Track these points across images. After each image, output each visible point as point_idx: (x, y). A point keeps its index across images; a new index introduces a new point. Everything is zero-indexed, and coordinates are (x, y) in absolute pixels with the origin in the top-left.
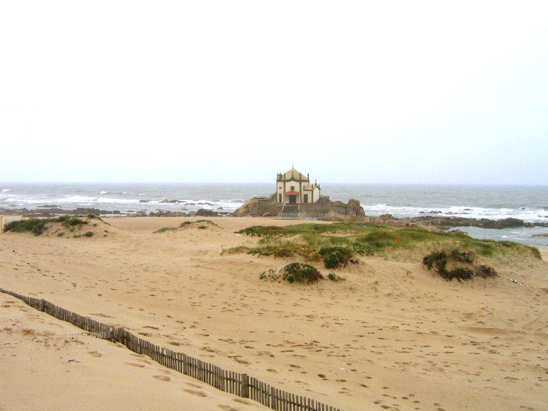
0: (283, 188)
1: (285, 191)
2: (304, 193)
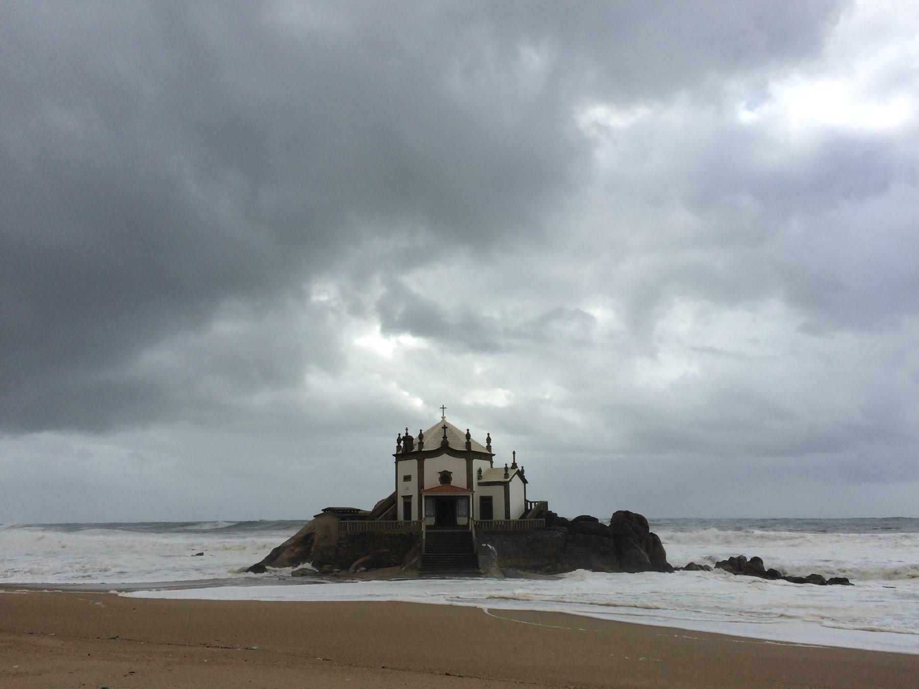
0: (415, 479)
1: (421, 485)
2: (478, 492)
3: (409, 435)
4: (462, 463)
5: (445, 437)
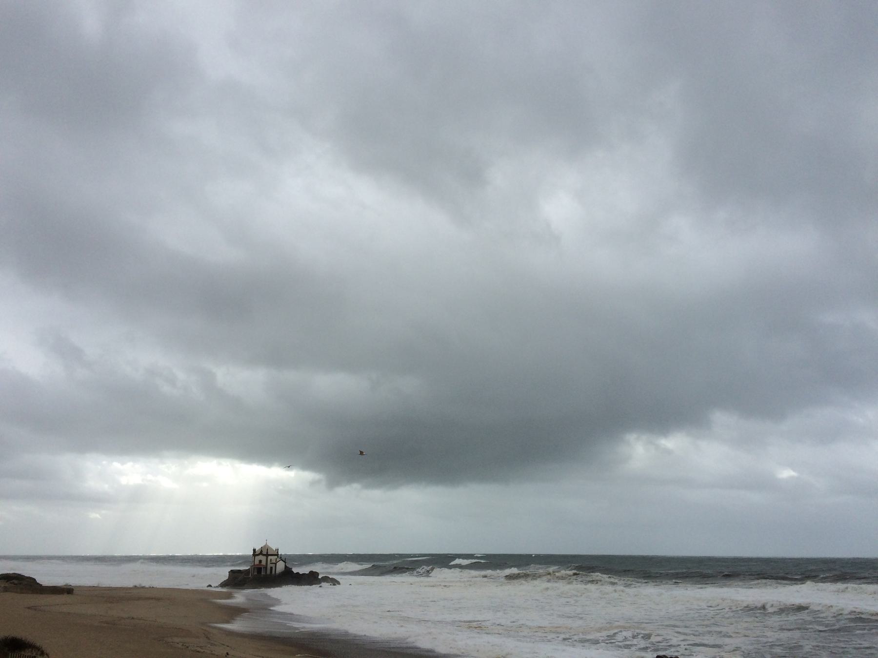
2: (269, 566)
4: (265, 557)
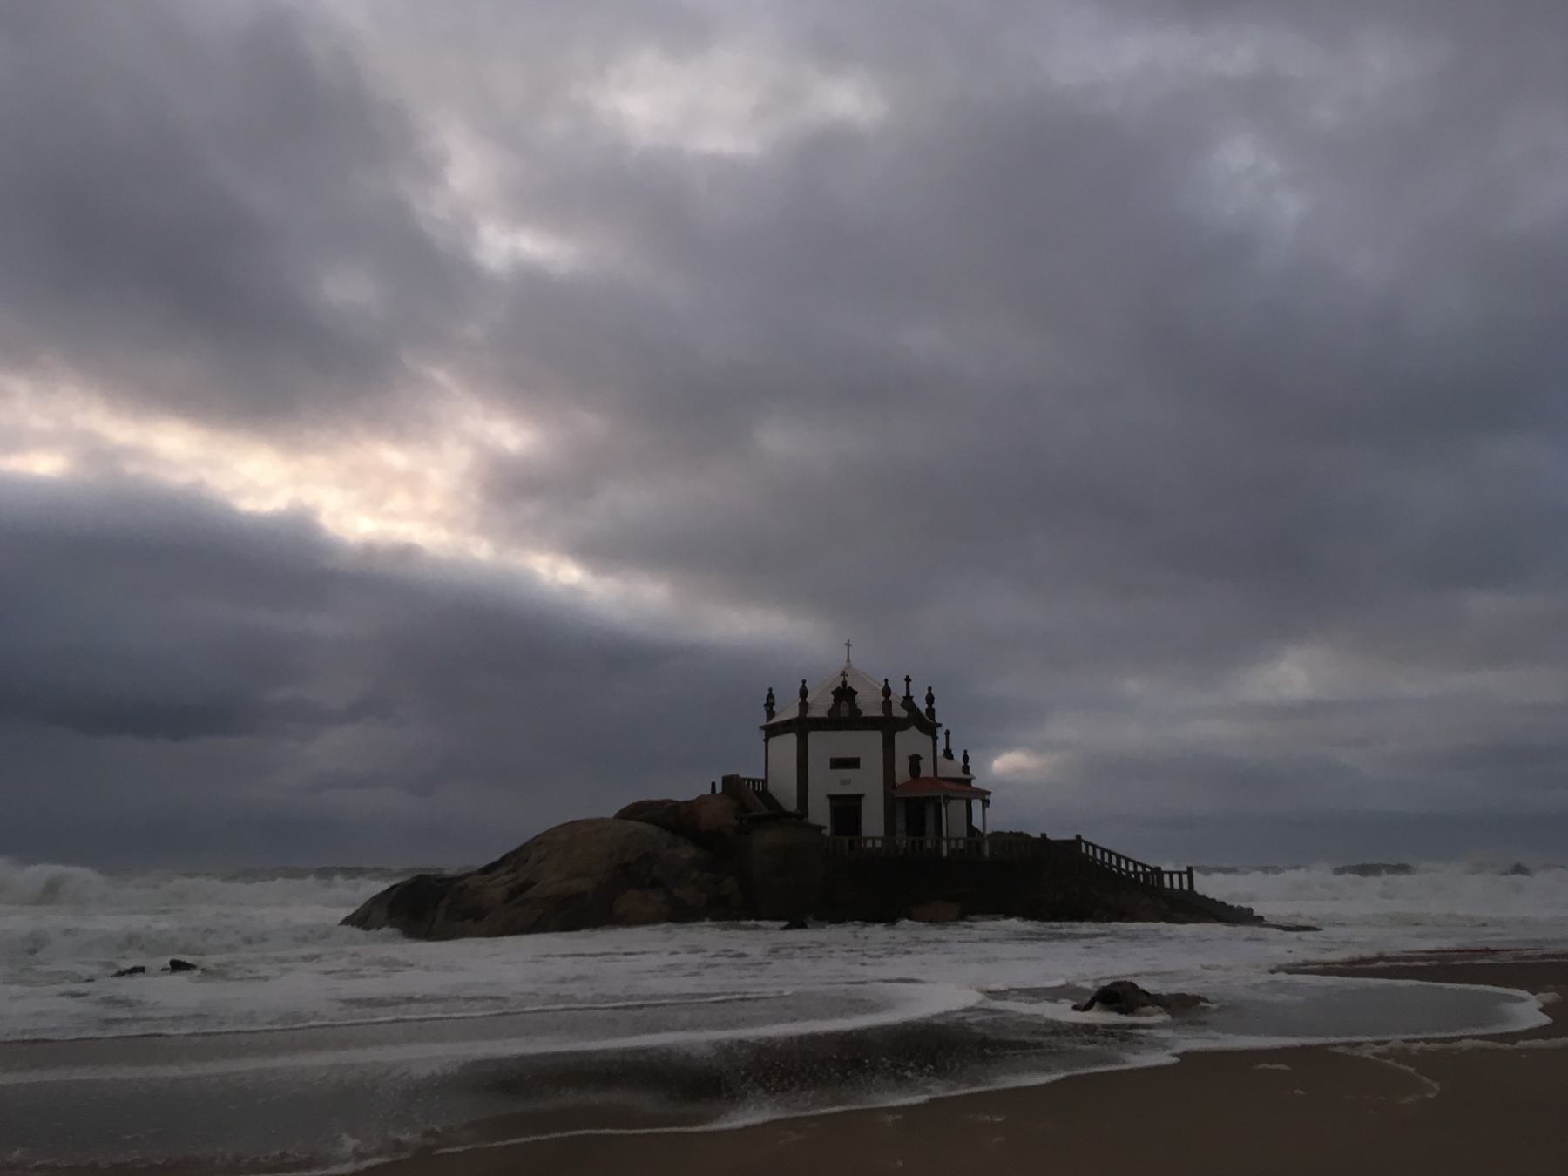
3: (848, 685)
5: (908, 698)
